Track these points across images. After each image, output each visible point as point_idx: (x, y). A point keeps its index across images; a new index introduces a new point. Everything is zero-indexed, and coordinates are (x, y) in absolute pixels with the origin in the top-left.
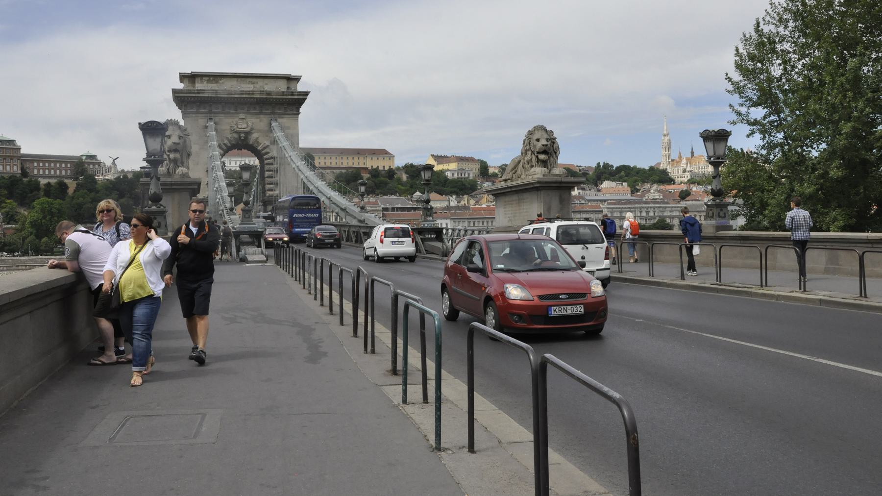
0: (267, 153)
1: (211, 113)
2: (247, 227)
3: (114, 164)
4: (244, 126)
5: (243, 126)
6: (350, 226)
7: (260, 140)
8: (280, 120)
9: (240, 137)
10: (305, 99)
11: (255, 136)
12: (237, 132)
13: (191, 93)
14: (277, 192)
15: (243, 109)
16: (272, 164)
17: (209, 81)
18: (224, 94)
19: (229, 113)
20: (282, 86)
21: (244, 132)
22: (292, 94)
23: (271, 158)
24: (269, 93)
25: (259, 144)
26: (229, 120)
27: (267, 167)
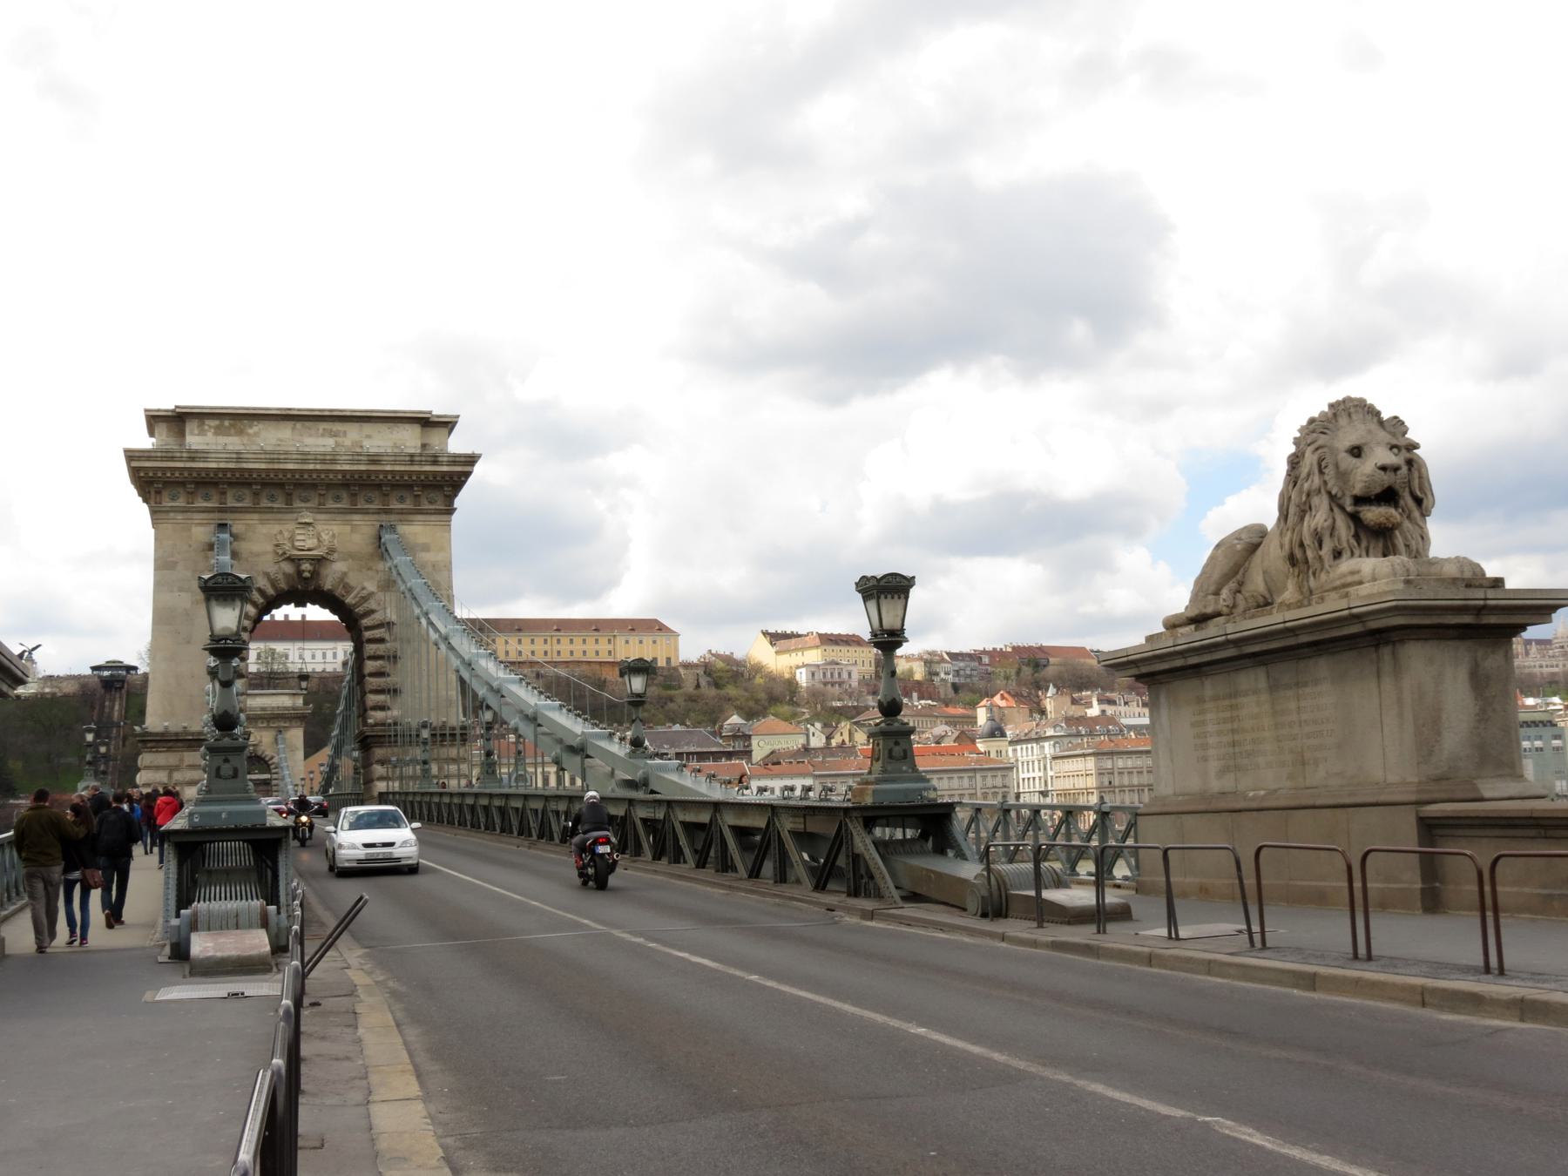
0: (373, 611)
1: (221, 510)
2: (225, 812)
4: (311, 543)
5: (306, 542)
7: (352, 580)
8: (403, 529)
9: (299, 572)
10: (468, 474)
11: (339, 567)
12: (290, 559)
13: (172, 459)
14: (395, 713)
15: (306, 500)
16: (381, 640)
17: (219, 431)
18: (257, 460)
19: (270, 510)
20: (409, 439)
24: (374, 459)
25: (348, 589)
26: (275, 528)
27: (370, 649)
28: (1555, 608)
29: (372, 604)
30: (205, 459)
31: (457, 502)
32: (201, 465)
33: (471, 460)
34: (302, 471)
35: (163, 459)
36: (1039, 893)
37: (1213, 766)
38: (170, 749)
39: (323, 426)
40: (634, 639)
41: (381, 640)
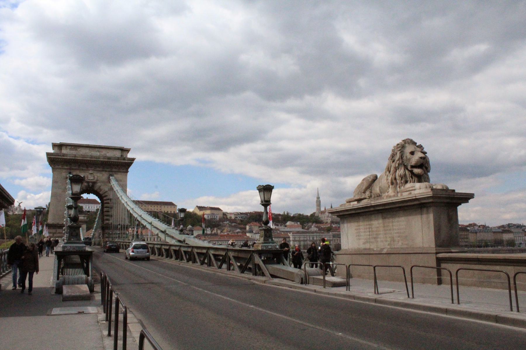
0: (107, 196)
1: (70, 169)
3: (19, 205)
4: (92, 178)
6: (171, 245)
7: (102, 187)
8: (115, 175)
9: (89, 185)
10: (132, 163)
11: (99, 184)
14: (111, 221)
15: (91, 167)
16: (108, 203)
17: (71, 149)
18: (80, 157)
19: (83, 170)
20: (118, 154)
21: (92, 182)
22: (124, 159)
23: (108, 199)
24: (109, 158)
25: (101, 190)
28: (469, 199)
29: (106, 194)
30: (67, 156)
31: (129, 170)
32: (65, 157)
33: (133, 159)
34: (91, 160)
35: (56, 155)
36: (324, 278)
37: (362, 241)
38: (54, 228)
39: (97, 149)
40: (166, 207)
41: (108, 203)
